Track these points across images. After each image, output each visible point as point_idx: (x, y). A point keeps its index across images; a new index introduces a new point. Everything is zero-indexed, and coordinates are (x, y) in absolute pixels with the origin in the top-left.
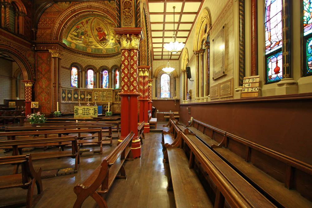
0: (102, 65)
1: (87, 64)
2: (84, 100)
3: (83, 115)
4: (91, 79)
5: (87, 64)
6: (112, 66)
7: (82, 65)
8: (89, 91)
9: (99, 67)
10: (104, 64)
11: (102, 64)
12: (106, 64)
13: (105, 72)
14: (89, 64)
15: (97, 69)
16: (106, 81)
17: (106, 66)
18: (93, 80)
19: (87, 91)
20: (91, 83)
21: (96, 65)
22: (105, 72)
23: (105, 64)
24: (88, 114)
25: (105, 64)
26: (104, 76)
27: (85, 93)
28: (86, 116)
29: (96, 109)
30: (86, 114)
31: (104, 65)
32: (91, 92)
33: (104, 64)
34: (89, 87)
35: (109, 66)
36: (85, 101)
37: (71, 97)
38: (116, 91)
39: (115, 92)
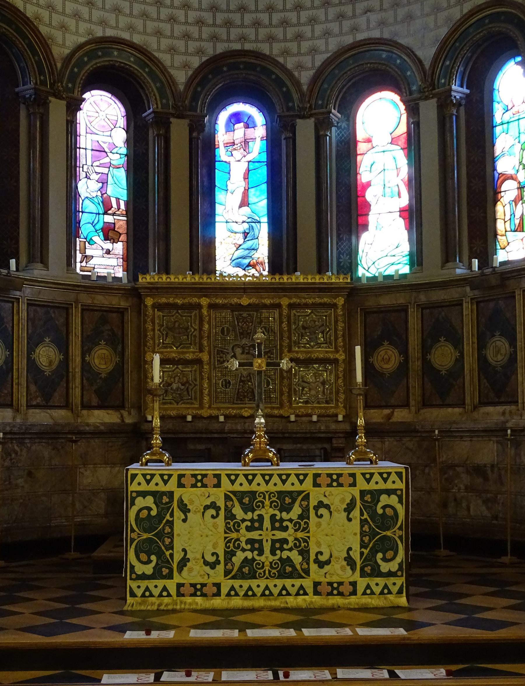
0: (221, 48)
1: (83, 27)
2: (57, 397)
3: (240, 575)
4: (104, 182)
5: (83, 27)
6: (319, 60)
7: (44, 30)
8: (101, 300)
9: (196, 62)
10: (243, 38)
11: (222, 32)
12: (263, 32)
13: (236, 117)
14: (99, 32)
15: (171, 81)
16: (245, 203)
17: (256, 55)
18: (123, 195)
19: (85, 299)
20: (109, 219)
21: (165, 43)
22: (236, 117)
23: (251, 33)
24: (296, 557)
25: (251, 33)
26: (221, 153)
27: (67, 324)
28: (267, 593)
29: (393, 500)
30: (267, 558)
31: (237, 46)
32: (121, 312)
33: (235, 33)
34: (87, 258)
35: (286, 53)
36: (67, 405)
37: (31, 350)
38: (385, 301)
39: (367, 313)
